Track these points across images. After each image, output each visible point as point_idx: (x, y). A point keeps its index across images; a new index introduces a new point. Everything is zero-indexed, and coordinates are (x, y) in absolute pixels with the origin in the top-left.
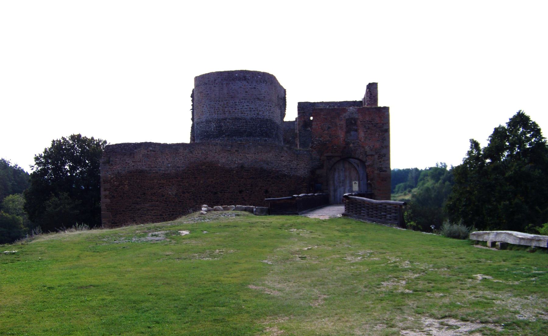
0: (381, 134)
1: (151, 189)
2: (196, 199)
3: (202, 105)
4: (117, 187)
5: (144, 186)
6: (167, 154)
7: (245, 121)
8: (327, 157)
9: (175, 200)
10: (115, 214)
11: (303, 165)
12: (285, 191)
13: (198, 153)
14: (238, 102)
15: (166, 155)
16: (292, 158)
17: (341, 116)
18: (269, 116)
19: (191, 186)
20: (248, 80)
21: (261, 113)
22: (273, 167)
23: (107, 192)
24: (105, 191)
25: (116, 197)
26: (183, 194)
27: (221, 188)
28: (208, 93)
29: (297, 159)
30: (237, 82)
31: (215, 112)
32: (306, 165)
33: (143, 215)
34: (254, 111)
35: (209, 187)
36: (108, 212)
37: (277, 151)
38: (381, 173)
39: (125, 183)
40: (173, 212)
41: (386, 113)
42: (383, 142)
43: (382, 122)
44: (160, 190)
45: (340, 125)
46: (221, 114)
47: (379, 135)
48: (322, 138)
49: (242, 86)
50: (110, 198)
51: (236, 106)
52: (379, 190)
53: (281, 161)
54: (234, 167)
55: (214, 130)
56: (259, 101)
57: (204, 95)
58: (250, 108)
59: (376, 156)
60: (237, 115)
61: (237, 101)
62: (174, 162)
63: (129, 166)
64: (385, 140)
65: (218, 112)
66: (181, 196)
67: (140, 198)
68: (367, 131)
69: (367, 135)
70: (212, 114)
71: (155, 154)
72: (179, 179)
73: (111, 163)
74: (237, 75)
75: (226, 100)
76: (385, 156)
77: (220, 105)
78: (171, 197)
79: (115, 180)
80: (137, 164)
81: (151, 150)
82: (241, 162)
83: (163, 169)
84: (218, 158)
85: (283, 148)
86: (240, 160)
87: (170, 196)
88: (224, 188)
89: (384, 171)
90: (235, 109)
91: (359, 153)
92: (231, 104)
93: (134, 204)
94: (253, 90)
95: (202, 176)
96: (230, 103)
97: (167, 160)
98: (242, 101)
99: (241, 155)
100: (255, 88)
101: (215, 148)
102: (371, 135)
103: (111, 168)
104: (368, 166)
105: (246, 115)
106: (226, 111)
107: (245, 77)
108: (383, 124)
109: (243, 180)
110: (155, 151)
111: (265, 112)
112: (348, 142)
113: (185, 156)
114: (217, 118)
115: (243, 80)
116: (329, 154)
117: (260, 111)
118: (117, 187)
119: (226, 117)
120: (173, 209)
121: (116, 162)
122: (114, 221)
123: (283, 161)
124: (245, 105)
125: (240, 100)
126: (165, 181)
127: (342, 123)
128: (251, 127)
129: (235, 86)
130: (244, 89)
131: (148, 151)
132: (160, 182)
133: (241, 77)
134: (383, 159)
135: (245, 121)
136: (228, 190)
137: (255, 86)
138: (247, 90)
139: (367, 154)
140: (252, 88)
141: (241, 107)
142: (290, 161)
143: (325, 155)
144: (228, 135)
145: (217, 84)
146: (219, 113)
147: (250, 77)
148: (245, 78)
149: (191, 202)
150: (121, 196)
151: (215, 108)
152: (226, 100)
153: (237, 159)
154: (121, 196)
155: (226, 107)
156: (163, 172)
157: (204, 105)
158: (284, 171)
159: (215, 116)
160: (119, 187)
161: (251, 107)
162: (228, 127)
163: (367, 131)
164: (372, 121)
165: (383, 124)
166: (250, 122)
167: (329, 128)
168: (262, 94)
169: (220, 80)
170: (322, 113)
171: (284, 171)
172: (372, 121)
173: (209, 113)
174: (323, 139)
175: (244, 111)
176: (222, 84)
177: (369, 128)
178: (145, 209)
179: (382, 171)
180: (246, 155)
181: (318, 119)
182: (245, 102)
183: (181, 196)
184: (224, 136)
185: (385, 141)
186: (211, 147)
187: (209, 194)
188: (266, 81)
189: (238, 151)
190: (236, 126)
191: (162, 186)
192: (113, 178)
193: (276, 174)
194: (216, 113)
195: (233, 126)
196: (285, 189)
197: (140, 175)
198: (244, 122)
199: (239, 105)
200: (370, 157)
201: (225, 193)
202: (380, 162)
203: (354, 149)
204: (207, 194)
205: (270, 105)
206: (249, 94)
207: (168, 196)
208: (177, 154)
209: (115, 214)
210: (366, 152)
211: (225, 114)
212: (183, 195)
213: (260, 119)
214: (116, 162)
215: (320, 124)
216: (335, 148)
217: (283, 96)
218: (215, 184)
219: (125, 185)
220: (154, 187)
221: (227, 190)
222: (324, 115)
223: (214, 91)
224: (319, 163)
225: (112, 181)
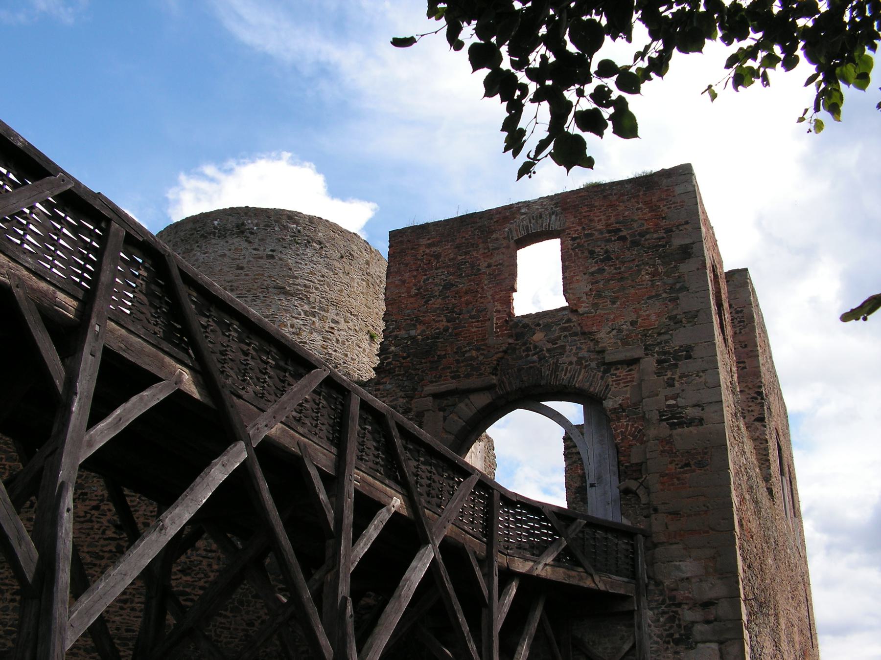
8: (436, 396)
17: (494, 236)
20: (252, 233)
38: (679, 430)
42: (674, 300)
45: (489, 266)
47: (654, 274)
49: (226, 252)
52: (675, 514)
56: (283, 297)
59: (650, 363)
64: (684, 288)
68: (601, 271)
69: (601, 285)
74: (216, 223)
76: (689, 357)
89: (690, 423)
91: (571, 363)
94: (262, 262)
104: (614, 410)
108: (669, 231)
115: (232, 234)
129: (206, 253)
130: (233, 259)
133: (229, 226)
134: (678, 372)
137: (272, 251)
139: (609, 358)
140: (261, 258)
147: (257, 225)
148: (241, 230)
163: (601, 271)
164: (620, 230)
170: (424, 241)
172: (620, 230)
174: (424, 331)
177: (608, 258)
179: (680, 424)
185: (680, 295)
188: (320, 243)
200: (622, 372)
203: (548, 350)
206: (247, 275)
210: (602, 352)
215: (415, 277)
216: (472, 358)
222: (429, 246)
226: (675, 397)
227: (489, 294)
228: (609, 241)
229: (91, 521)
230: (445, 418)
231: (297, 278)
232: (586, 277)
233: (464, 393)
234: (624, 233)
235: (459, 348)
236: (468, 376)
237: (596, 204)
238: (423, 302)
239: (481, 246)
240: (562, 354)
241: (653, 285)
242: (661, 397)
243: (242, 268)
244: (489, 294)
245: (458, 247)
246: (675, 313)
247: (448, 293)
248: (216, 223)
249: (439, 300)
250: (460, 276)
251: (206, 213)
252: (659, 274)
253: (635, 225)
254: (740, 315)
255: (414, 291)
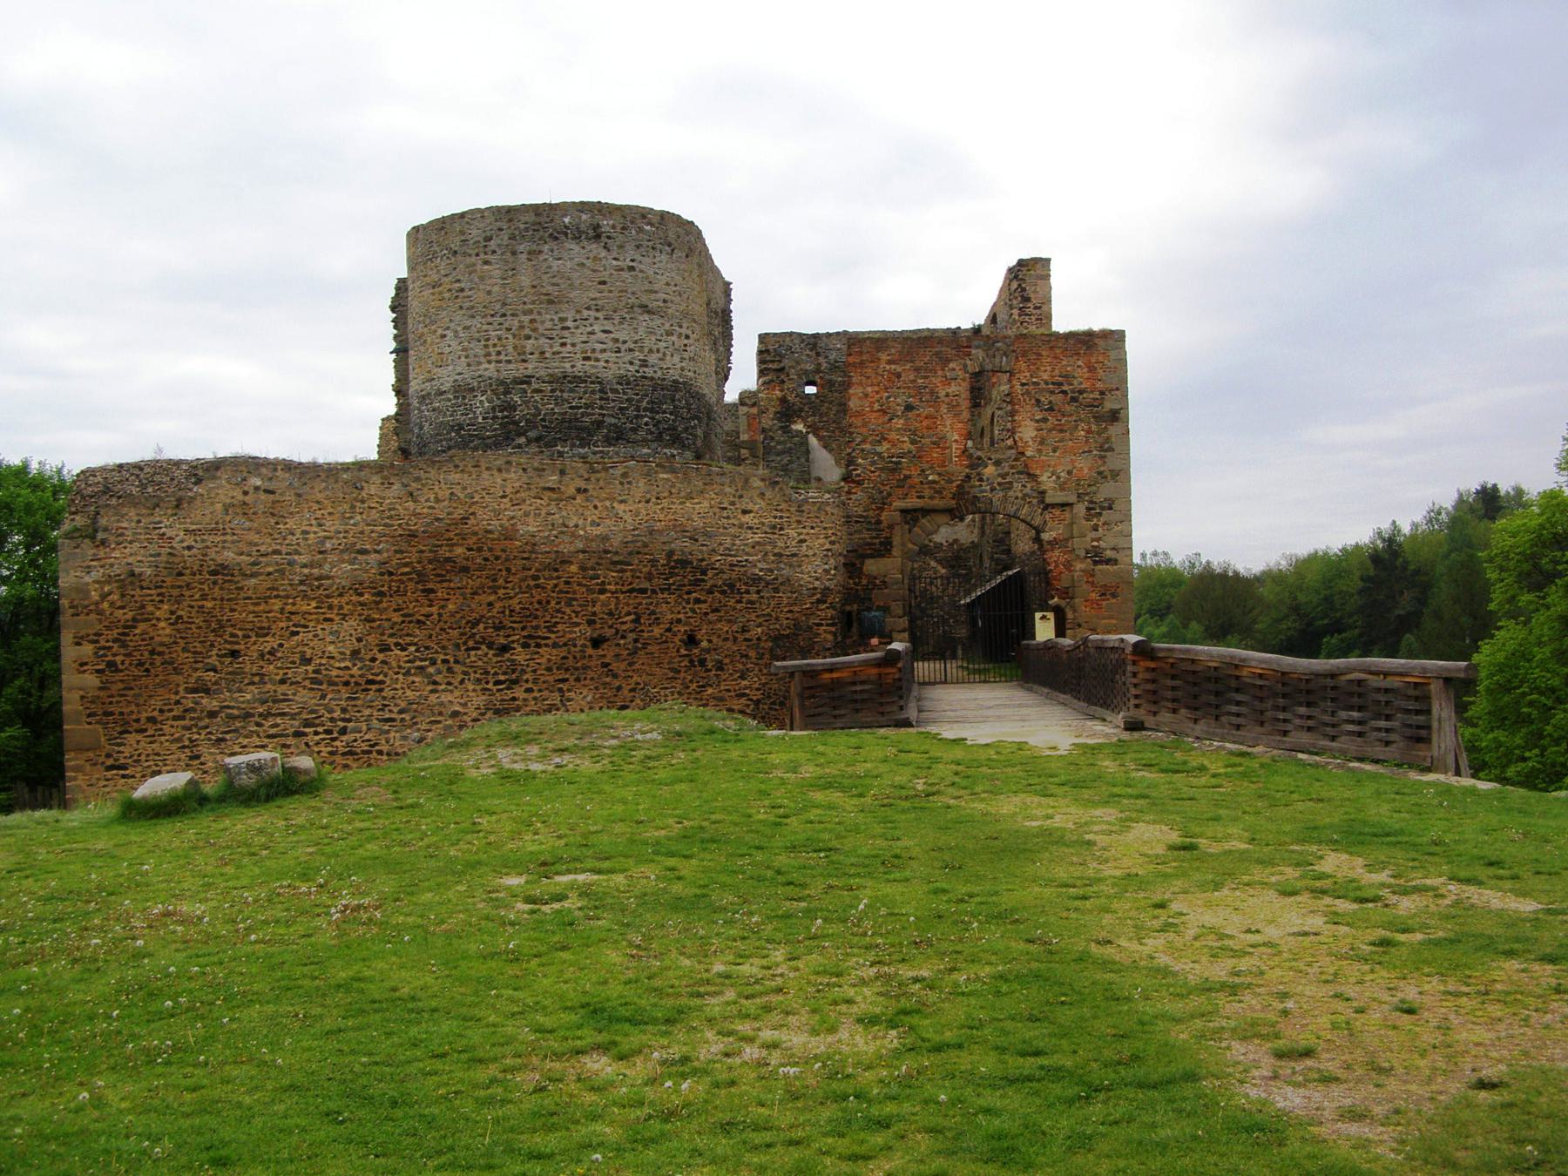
0: (1094, 428)
1: (257, 636)
2: (431, 670)
3: (440, 331)
4: (125, 627)
5: (232, 626)
6: (318, 502)
7: (598, 387)
8: (904, 511)
9: (352, 676)
10: (121, 733)
11: (820, 541)
12: (759, 639)
13: (437, 500)
14: (570, 319)
15: (316, 506)
16: (781, 517)
18: (682, 369)
19: (410, 622)
20: (609, 237)
21: (653, 359)
22: (714, 550)
23: (88, 649)
24: (78, 644)
25: (120, 667)
26: (381, 651)
27: (523, 629)
28: (462, 285)
29: (799, 522)
30: (571, 245)
31: (489, 354)
32: (832, 543)
33: (228, 737)
34: (631, 350)
35: (481, 626)
36: (90, 723)
37: (728, 489)
39: (158, 613)
40: (344, 720)
41: (1113, 354)
43: (1099, 385)
44: (296, 638)
45: (947, 395)
46: (509, 362)
47: (1089, 432)
48: (886, 446)
50: (98, 671)
51: (566, 333)
53: (741, 526)
54: (572, 549)
55: (484, 418)
56: (646, 317)
57: (447, 295)
58: (617, 340)
59: (1080, 509)
60: (568, 365)
61: (570, 315)
62: (346, 532)
63: (172, 548)
64: (1111, 449)
65: (499, 353)
66: (373, 660)
67: (215, 671)
68: (1045, 420)
70: (479, 363)
71: (274, 502)
72: (366, 596)
73: (100, 536)
74: (567, 220)
75: (531, 312)
76: (1110, 508)
77: (508, 330)
78: (337, 665)
79: (119, 604)
80: (203, 541)
81: (257, 489)
82: (597, 531)
83: (303, 559)
84: (513, 518)
85: (747, 481)
86: (593, 523)
87: (332, 662)
88: (537, 628)
89: (1108, 561)
90: (563, 345)
91: (1017, 498)
92: (548, 325)
93: (195, 691)
94: (625, 275)
95: (452, 585)
96: (543, 322)
97: (320, 525)
98: (586, 313)
99: (596, 507)
100: (632, 269)
101: (499, 481)
102: (1062, 431)
103: (102, 554)
104: (1049, 542)
105: (602, 364)
106: (528, 350)
107: (597, 227)
108: (1102, 393)
109: (602, 597)
110: (272, 492)
111: (668, 358)
112: (979, 458)
113: (390, 510)
114: (495, 375)
116: (912, 502)
117: (651, 351)
118: (125, 627)
119: (529, 372)
120: (344, 710)
121: (122, 535)
122: (116, 760)
123: (751, 528)
124: (596, 328)
125: (578, 312)
126: (314, 604)
127: (953, 389)
128: (621, 409)
129: (559, 259)
130: (594, 271)
131: (246, 493)
132: (293, 609)
133: (583, 227)
135: (598, 387)
136: (553, 636)
137: (632, 261)
138: (605, 276)
139: (1048, 500)
140: (622, 270)
141: (584, 338)
142: (774, 527)
143: (898, 504)
144: (538, 439)
145: (494, 252)
146: (502, 357)
147: (614, 227)
148: (597, 235)
149: (413, 682)
150: (141, 664)
151: (488, 340)
152: (531, 312)
153: (580, 522)
154: (141, 664)
155: (528, 337)
156: (306, 571)
157: (448, 328)
158: (755, 566)
159: (489, 370)
160: (135, 627)
161: (622, 336)
162: (536, 408)
163: (1045, 420)
164: (1061, 384)
165: (1102, 393)
166: (615, 391)
167: (909, 408)
168: (656, 292)
169: (506, 238)
170: (884, 357)
171: (755, 566)
172: (1061, 384)
173: (467, 357)
175: (594, 351)
176: (514, 253)
177: (1051, 409)
178: (236, 712)
179: (1100, 562)
180: (615, 505)
181: (868, 378)
182: (597, 319)
183: (373, 660)
184: (522, 440)
185: (1108, 454)
186: (485, 475)
187: (479, 652)
188: (669, 245)
189: (586, 491)
190: (567, 405)
191: (303, 622)
192: (110, 593)
193: (725, 576)
194: (494, 358)
195: (556, 404)
196: (759, 630)
197: (215, 583)
198: (593, 392)
199: (577, 328)
200: (1057, 512)
201: (538, 646)
202: (1095, 528)
203: (999, 484)
204: (473, 653)
205: (684, 331)
206: (611, 292)
207: (324, 661)
208: (358, 504)
209: (121, 733)
210: (1043, 493)
211: (524, 361)
212: (381, 657)
213: (652, 379)
214: (122, 535)
215: (877, 393)
216: (934, 482)
217: (722, 303)
218: (503, 612)
219: (158, 619)
220: (269, 628)
221: (549, 638)
222: (889, 362)
223: (482, 279)
224: (874, 534)
225: (105, 605)
226: (1098, 540)
227: (948, 423)
228: (1052, 392)
229: (666, 642)
230: (910, 531)
231: (656, 292)
232: (1033, 423)
233: (926, 512)
234: (1065, 388)
235: (923, 471)
236: (931, 498)
237: (1044, 353)
238: (887, 418)
239: (940, 373)
240: (1010, 488)
241: (1087, 442)
242: (1088, 539)
243: (604, 283)
244: (948, 423)
245: (917, 370)
246: (1102, 469)
247: (910, 415)
248: (567, 220)
249: (902, 421)
250: (921, 401)
251: (550, 205)
252: (1092, 432)
253: (1075, 382)
254: (1038, 311)
255: (877, 407)
